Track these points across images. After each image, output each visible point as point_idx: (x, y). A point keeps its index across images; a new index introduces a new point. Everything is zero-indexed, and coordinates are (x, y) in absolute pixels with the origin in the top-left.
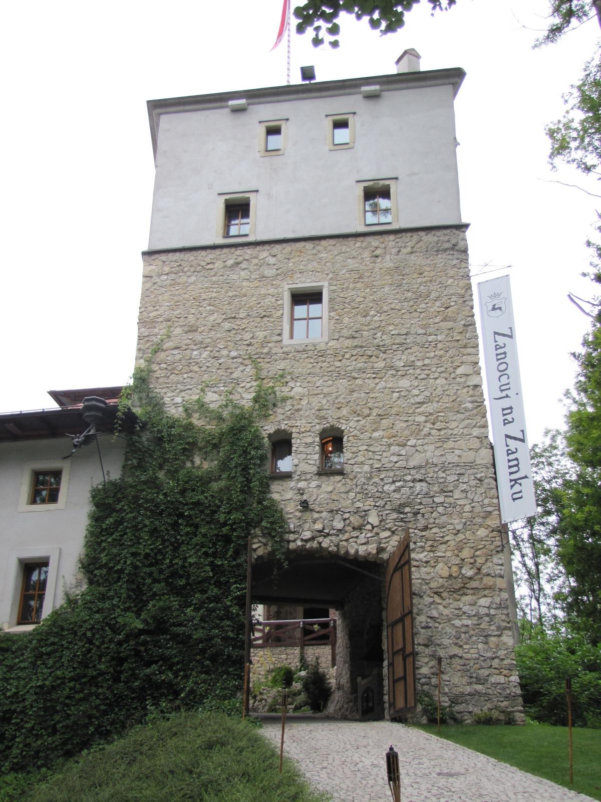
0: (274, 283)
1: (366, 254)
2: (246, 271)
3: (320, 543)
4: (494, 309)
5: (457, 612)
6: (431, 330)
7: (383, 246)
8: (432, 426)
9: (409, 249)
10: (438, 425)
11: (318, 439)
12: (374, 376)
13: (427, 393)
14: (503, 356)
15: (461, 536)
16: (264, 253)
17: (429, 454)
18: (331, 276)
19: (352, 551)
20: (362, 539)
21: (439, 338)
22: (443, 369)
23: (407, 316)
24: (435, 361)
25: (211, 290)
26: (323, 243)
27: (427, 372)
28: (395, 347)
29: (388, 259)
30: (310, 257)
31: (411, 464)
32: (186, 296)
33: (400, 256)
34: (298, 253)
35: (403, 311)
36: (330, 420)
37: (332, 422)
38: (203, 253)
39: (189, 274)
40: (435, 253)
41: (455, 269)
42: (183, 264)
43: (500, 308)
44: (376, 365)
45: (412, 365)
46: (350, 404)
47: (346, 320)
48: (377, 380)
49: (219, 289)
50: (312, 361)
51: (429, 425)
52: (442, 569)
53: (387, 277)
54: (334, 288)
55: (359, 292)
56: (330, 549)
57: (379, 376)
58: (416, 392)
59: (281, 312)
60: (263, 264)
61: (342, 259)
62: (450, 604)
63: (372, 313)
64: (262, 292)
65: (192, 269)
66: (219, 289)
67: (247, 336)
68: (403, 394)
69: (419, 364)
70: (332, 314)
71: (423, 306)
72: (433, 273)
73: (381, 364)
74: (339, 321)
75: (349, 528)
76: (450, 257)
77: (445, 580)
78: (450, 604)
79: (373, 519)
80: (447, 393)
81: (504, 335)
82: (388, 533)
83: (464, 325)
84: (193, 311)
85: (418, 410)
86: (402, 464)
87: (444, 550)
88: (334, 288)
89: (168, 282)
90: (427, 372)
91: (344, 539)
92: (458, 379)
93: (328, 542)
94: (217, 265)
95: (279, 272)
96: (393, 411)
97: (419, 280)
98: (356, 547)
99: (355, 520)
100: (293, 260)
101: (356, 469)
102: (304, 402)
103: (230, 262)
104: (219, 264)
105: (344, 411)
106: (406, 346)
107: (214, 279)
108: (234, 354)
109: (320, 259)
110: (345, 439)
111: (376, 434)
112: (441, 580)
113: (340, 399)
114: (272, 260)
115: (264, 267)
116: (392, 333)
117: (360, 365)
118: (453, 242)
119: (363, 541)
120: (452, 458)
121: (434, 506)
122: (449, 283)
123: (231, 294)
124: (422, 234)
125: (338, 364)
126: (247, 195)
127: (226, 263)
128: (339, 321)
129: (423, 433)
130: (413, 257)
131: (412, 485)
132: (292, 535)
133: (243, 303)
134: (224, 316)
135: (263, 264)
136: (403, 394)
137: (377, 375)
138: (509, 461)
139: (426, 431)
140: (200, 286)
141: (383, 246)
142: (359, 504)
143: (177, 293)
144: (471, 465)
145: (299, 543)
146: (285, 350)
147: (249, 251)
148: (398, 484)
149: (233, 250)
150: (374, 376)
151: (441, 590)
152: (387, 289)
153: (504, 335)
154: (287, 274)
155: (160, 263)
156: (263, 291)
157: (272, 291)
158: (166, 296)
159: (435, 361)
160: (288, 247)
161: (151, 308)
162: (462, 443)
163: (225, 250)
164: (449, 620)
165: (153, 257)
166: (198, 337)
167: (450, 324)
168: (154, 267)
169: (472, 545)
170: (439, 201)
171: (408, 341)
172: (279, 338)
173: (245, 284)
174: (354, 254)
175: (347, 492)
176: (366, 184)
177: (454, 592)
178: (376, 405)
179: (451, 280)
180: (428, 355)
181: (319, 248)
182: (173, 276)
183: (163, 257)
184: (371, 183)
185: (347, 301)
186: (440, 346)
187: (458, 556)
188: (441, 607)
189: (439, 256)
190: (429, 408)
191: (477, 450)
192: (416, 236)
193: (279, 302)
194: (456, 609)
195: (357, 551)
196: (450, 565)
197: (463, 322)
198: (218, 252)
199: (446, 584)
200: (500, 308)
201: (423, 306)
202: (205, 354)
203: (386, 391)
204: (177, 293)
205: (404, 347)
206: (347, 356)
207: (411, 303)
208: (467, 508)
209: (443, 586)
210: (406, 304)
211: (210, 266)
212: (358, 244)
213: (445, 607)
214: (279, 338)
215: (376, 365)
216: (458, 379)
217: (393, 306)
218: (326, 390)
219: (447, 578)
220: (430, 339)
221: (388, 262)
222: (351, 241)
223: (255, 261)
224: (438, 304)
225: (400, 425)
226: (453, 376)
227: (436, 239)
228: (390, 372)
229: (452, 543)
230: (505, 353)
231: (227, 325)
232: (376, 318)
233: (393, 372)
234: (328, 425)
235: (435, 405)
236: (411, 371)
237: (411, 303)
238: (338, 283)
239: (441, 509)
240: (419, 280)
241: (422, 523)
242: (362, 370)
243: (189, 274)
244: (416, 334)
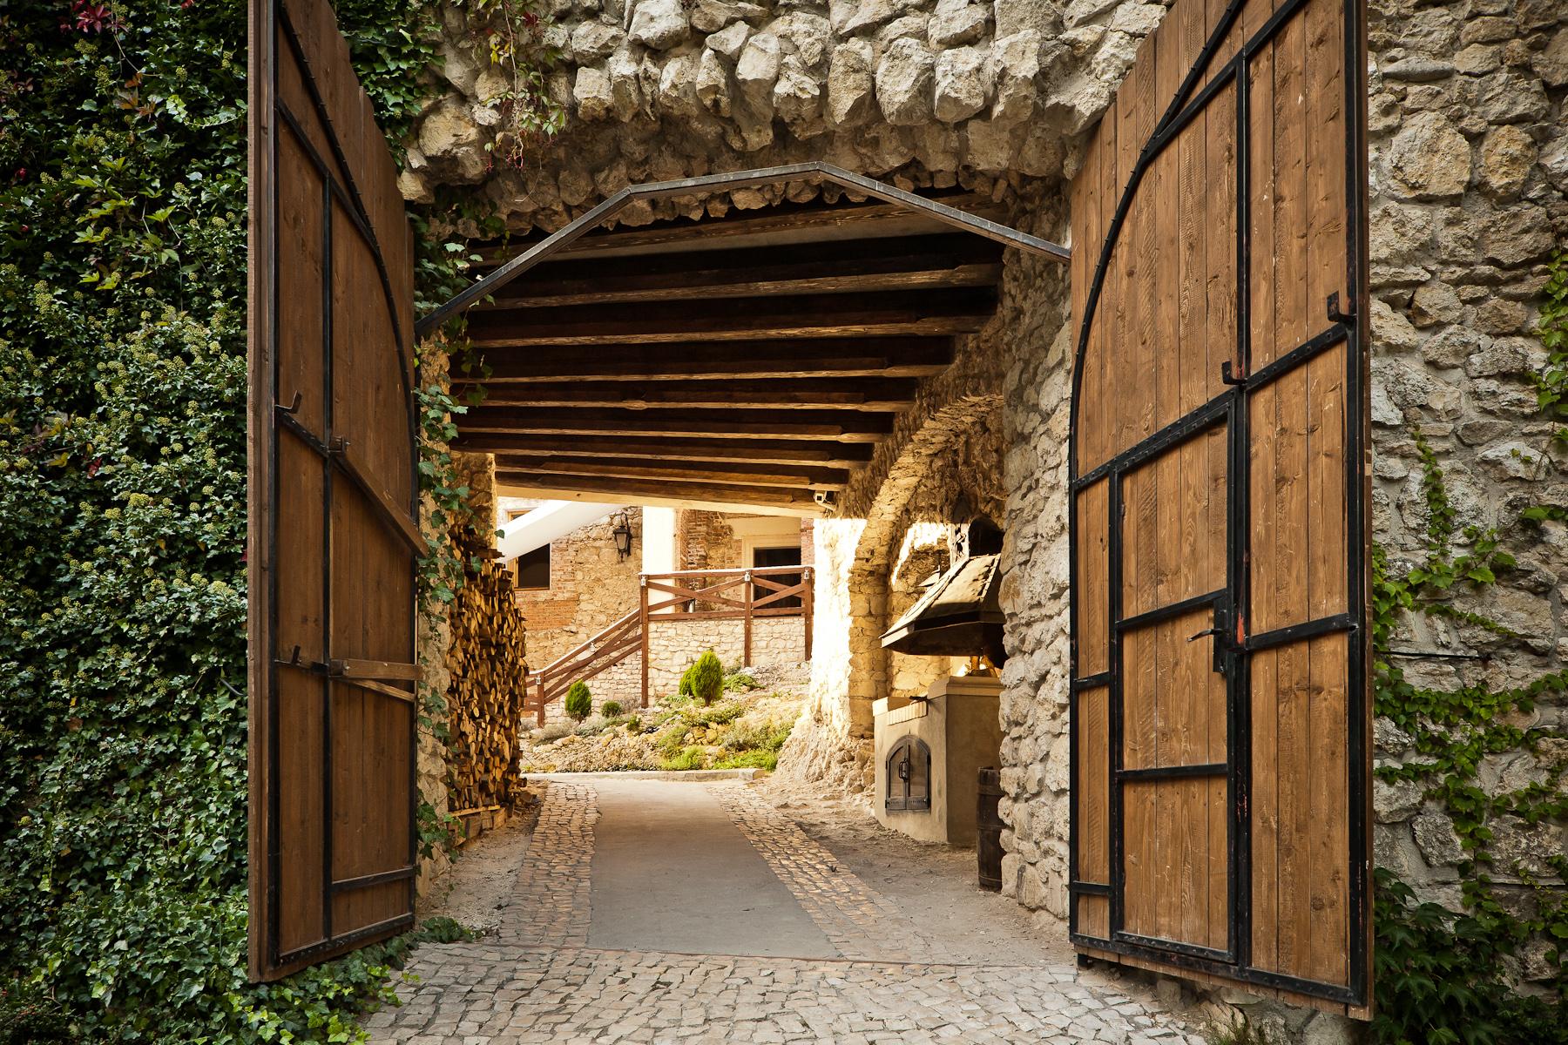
3: (729, 62)
5: (1512, 392)
19: (897, 89)
52: (1432, 150)
56: (782, 88)
62: (1467, 350)
77: (1444, 212)
78: (1467, 350)
87: (1442, 36)
91: (853, 23)
93: (773, 45)
98: (919, 56)
112: (1416, 213)
119: (959, 27)
132: (585, 28)
151: (1413, 272)
164: (1468, 439)
177: (1491, 281)
187: (1525, 69)
188: (1414, 370)
194: (1505, 377)
195: (926, 87)
196: (1474, 123)
199: (1447, 237)
209: (1428, 248)
213: (1433, 365)
219: (1454, 200)
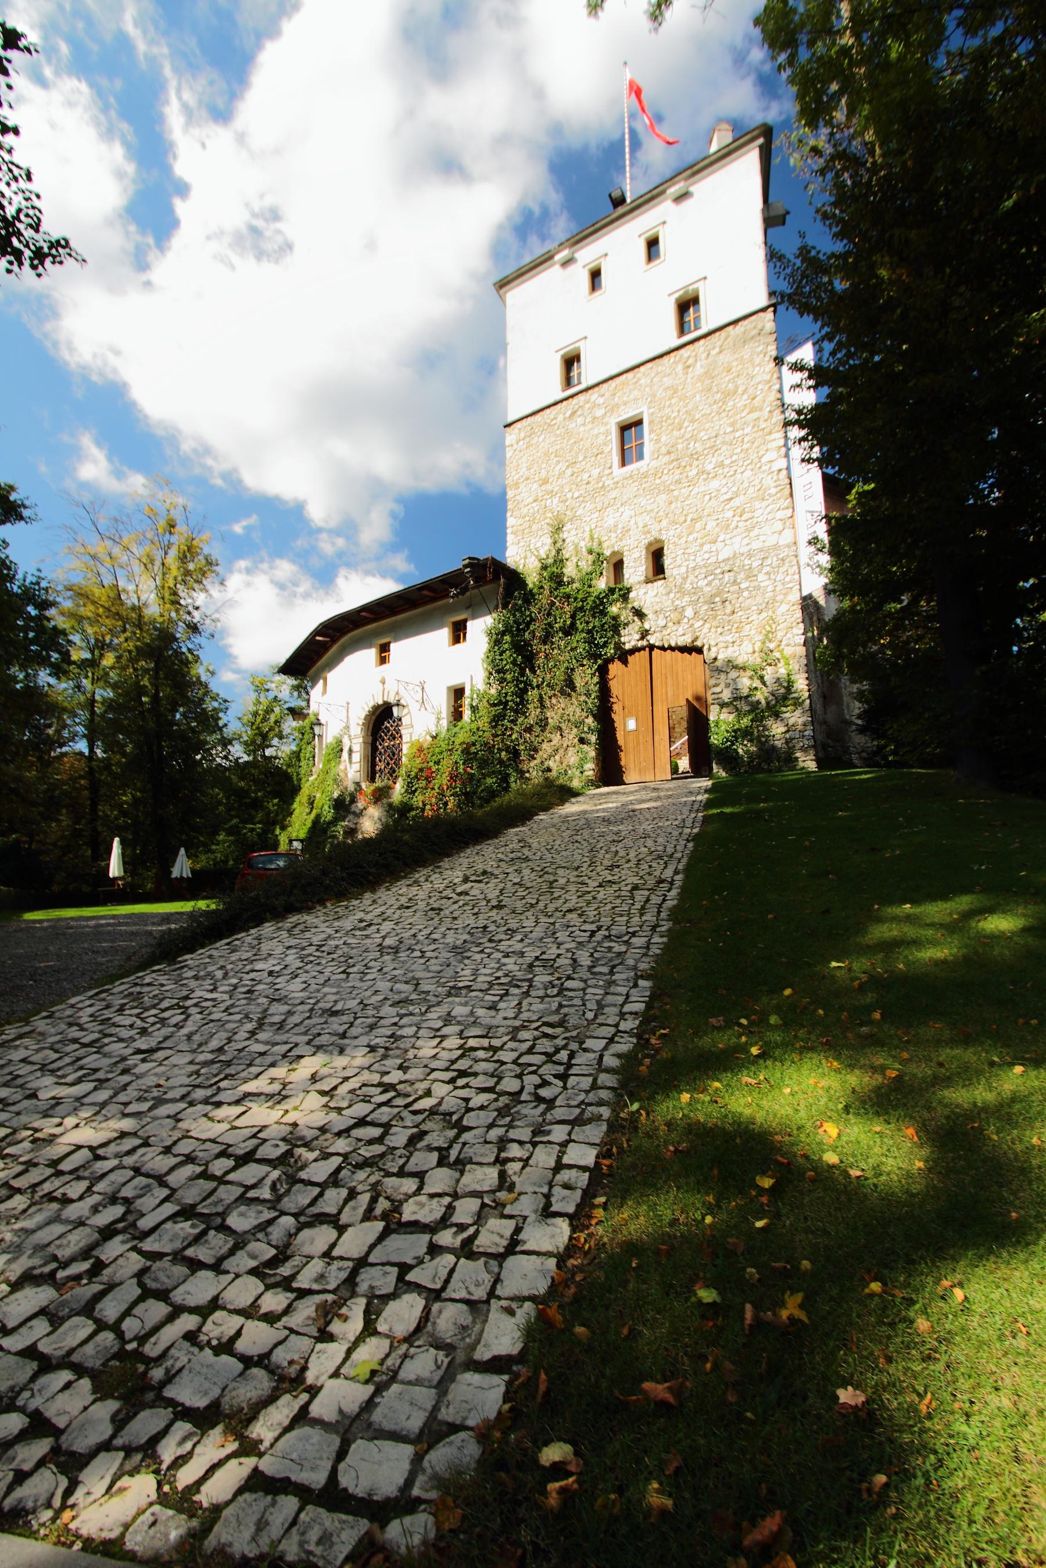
1: (680, 367)
9: (717, 350)
13: (735, 489)
15: (764, 615)
16: (593, 395)
17: (736, 546)
20: (681, 631)
24: (742, 455)
26: (642, 369)
31: (721, 559)
33: (710, 359)
37: (655, 534)
45: (721, 465)
47: (664, 438)
51: (737, 518)
60: (595, 406)
67: (585, 476)
71: (731, 403)
73: (695, 472)
75: (670, 624)
79: (689, 612)
82: (701, 623)
86: (713, 559)
96: (706, 513)
99: (674, 616)
101: (675, 572)
102: (632, 522)
104: (561, 417)
105: (664, 523)
108: (576, 495)
111: (691, 538)
113: (661, 513)
114: (601, 400)
118: (759, 327)
120: (756, 545)
121: (740, 591)
125: (658, 481)
128: (658, 441)
130: (721, 357)
135: (595, 406)
137: (692, 483)
142: (677, 602)
144: (776, 547)
145: (633, 643)
147: (581, 398)
148: (710, 578)
152: (698, 398)
154: (612, 409)
156: (596, 431)
158: (524, 459)
159: (742, 455)
160: (613, 384)
162: (767, 530)
166: (549, 487)
167: (755, 415)
173: (582, 429)
174: (668, 371)
175: (668, 594)
181: (639, 375)
183: (519, 425)
190: (736, 503)
191: (780, 532)
192: (723, 333)
198: (559, 406)
202: (556, 500)
205: (714, 449)
208: (770, 588)
218: (649, 508)
222: (666, 359)
223: (587, 406)
224: (745, 397)
225: (711, 525)
229: (756, 623)
231: (569, 472)
239: (746, 594)
241: (729, 608)
242: (678, 482)
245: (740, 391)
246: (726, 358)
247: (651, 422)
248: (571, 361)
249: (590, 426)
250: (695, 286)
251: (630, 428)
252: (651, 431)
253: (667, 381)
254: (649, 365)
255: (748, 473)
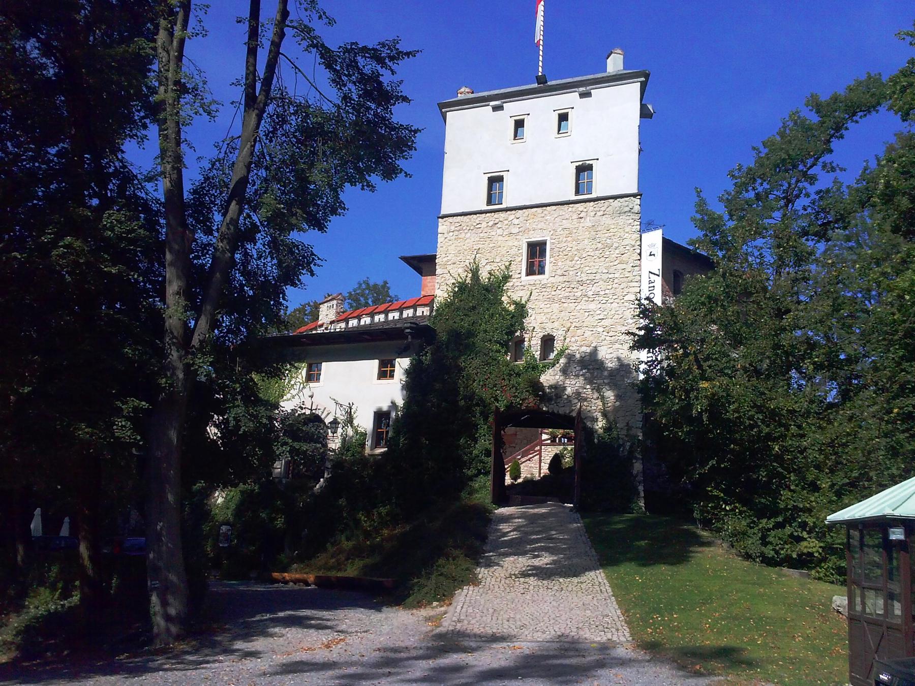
0: (517, 237)
1: (575, 216)
2: (501, 229)
4: (650, 255)
6: (611, 270)
7: (585, 210)
8: (607, 334)
9: (602, 213)
10: (611, 334)
11: (540, 342)
12: (575, 301)
14: (653, 288)
16: (511, 215)
18: (551, 233)
21: (616, 276)
22: (616, 297)
23: (597, 260)
24: (612, 291)
25: (479, 242)
27: (607, 299)
28: (588, 282)
29: (588, 220)
30: (540, 219)
32: (465, 247)
33: (597, 218)
34: (533, 216)
35: (595, 257)
36: (547, 329)
38: (475, 216)
39: (466, 231)
40: (619, 215)
41: (630, 227)
42: (462, 224)
43: (654, 255)
44: (576, 294)
46: (559, 320)
47: (560, 264)
48: (576, 304)
49: (484, 242)
50: (538, 291)
51: (605, 333)
53: (587, 233)
54: (554, 241)
55: (569, 244)
57: (577, 301)
58: (599, 312)
59: (521, 258)
60: (511, 223)
61: (559, 220)
63: (576, 258)
64: (510, 245)
65: (468, 229)
66: (484, 242)
68: (591, 313)
69: (602, 293)
70: (552, 259)
72: (616, 230)
73: (579, 294)
74: (555, 264)
76: (628, 218)
80: (617, 313)
81: (654, 274)
83: (632, 266)
84: (468, 257)
85: (599, 324)
88: (554, 241)
89: (454, 237)
90: (607, 299)
92: (625, 304)
94: (483, 224)
95: (520, 229)
97: (606, 235)
100: (529, 221)
103: (491, 224)
104: (484, 225)
105: (556, 325)
106: (595, 281)
107: (482, 235)
109: (546, 220)
110: (555, 342)
111: (573, 339)
114: (516, 221)
115: (512, 226)
116: (587, 272)
117: (567, 294)
122: (625, 237)
123: (491, 245)
124: (611, 201)
125: (553, 293)
126: (501, 174)
127: (488, 224)
129: (601, 339)
131: (592, 371)
133: (498, 252)
134: (487, 261)
135: (511, 223)
136: (591, 313)
138: (648, 357)
139: (603, 337)
140: (473, 240)
141: (585, 210)
143: (459, 245)
146: (523, 284)
147: (502, 215)
149: (493, 214)
150: (575, 301)
152: (586, 241)
153: (654, 274)
155: (449, 224)
156: (510, 243)
157: (516, 243)
158: (453, 247)
161: (444, 255)
163: (488, 215)
165: (445, 219)
167: (624, 266)
168: (444, 227)
169: (624, 409)
170: (624, 176)
171: (596, 278)
172: (519, 276)
173: (500, 238)
176: (578, 164)
178: (574, 320)
179: (627, 235)
180: (608, 287)
181: (545, 212)
182: (456, 233)
183: (450, 219)
184: (581, 163)
185: (561, 250)
186: (616, 281)
189: (621, 217)
192: (607, 202)
193: (520, 251)
197: (632, 265)
198: (483, 215)
200: (654, 255)
201: (608, 253)
203: (582, 311)
204: (459, 245)
205: (593, 282)
206: (559, 288)
207: (601, 251)
210: (597, 252)
211: (477, 227)
212: (570, 209)
214: (519, 276)
215: (576, 294)
216: (625, 304)
217: (589, 253)
220: (610, 276)
221: (588, 223)
223: (506, 222)
224: (617, 251)
225: (588, 334)
226: (622, 301)
227: (620, 204)
228: (584, 299)
230: (654, 287)
232: (578, 262)
233: (587, 299)
234: (546, 333)
235: (610, 320)
236: (597, 298)
237: (601, 251)
238: (556, 237)
240: (606, 235)
242: (568, 298)
243: (466, 231)
244: (602, 273)
245: (616, 245)
246: (607, 220)
247: (552, 249)
248: (495, 181)
249: (507, 238)
250: (590, 162)
251: (536, 251)
252: (552, 256)
253: (566, 224)
254: (554, 208)
255: (615, 305)
